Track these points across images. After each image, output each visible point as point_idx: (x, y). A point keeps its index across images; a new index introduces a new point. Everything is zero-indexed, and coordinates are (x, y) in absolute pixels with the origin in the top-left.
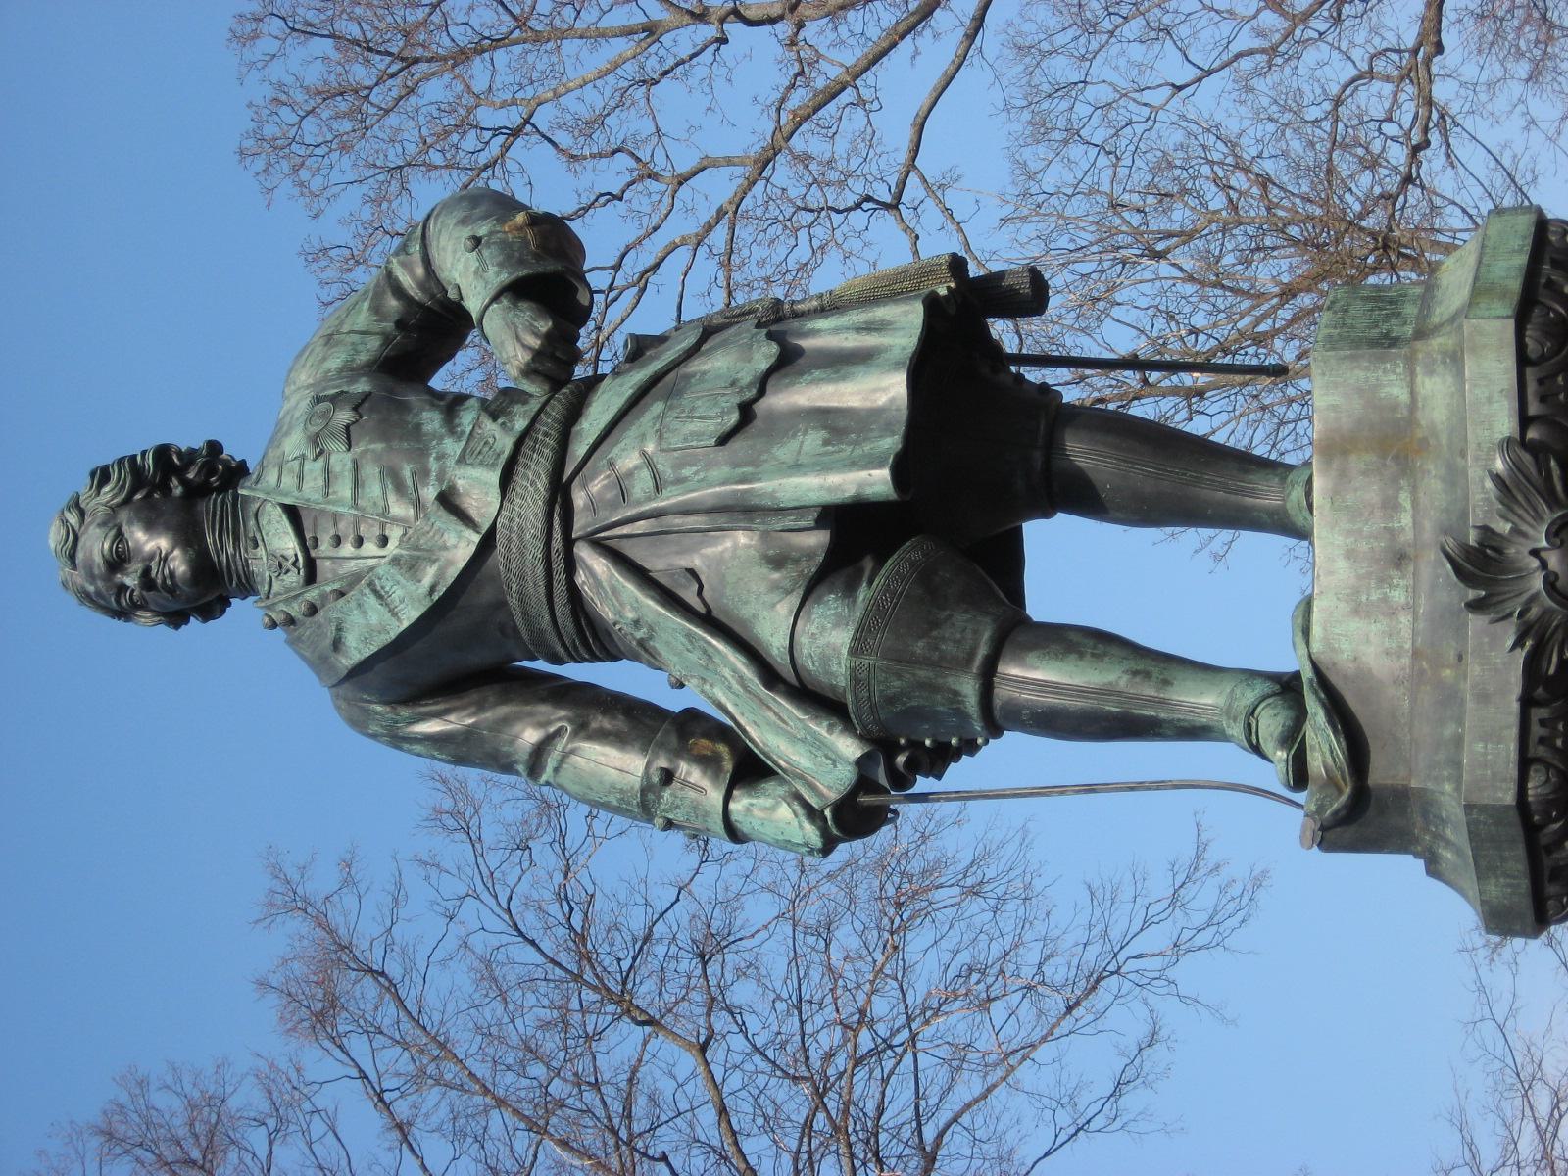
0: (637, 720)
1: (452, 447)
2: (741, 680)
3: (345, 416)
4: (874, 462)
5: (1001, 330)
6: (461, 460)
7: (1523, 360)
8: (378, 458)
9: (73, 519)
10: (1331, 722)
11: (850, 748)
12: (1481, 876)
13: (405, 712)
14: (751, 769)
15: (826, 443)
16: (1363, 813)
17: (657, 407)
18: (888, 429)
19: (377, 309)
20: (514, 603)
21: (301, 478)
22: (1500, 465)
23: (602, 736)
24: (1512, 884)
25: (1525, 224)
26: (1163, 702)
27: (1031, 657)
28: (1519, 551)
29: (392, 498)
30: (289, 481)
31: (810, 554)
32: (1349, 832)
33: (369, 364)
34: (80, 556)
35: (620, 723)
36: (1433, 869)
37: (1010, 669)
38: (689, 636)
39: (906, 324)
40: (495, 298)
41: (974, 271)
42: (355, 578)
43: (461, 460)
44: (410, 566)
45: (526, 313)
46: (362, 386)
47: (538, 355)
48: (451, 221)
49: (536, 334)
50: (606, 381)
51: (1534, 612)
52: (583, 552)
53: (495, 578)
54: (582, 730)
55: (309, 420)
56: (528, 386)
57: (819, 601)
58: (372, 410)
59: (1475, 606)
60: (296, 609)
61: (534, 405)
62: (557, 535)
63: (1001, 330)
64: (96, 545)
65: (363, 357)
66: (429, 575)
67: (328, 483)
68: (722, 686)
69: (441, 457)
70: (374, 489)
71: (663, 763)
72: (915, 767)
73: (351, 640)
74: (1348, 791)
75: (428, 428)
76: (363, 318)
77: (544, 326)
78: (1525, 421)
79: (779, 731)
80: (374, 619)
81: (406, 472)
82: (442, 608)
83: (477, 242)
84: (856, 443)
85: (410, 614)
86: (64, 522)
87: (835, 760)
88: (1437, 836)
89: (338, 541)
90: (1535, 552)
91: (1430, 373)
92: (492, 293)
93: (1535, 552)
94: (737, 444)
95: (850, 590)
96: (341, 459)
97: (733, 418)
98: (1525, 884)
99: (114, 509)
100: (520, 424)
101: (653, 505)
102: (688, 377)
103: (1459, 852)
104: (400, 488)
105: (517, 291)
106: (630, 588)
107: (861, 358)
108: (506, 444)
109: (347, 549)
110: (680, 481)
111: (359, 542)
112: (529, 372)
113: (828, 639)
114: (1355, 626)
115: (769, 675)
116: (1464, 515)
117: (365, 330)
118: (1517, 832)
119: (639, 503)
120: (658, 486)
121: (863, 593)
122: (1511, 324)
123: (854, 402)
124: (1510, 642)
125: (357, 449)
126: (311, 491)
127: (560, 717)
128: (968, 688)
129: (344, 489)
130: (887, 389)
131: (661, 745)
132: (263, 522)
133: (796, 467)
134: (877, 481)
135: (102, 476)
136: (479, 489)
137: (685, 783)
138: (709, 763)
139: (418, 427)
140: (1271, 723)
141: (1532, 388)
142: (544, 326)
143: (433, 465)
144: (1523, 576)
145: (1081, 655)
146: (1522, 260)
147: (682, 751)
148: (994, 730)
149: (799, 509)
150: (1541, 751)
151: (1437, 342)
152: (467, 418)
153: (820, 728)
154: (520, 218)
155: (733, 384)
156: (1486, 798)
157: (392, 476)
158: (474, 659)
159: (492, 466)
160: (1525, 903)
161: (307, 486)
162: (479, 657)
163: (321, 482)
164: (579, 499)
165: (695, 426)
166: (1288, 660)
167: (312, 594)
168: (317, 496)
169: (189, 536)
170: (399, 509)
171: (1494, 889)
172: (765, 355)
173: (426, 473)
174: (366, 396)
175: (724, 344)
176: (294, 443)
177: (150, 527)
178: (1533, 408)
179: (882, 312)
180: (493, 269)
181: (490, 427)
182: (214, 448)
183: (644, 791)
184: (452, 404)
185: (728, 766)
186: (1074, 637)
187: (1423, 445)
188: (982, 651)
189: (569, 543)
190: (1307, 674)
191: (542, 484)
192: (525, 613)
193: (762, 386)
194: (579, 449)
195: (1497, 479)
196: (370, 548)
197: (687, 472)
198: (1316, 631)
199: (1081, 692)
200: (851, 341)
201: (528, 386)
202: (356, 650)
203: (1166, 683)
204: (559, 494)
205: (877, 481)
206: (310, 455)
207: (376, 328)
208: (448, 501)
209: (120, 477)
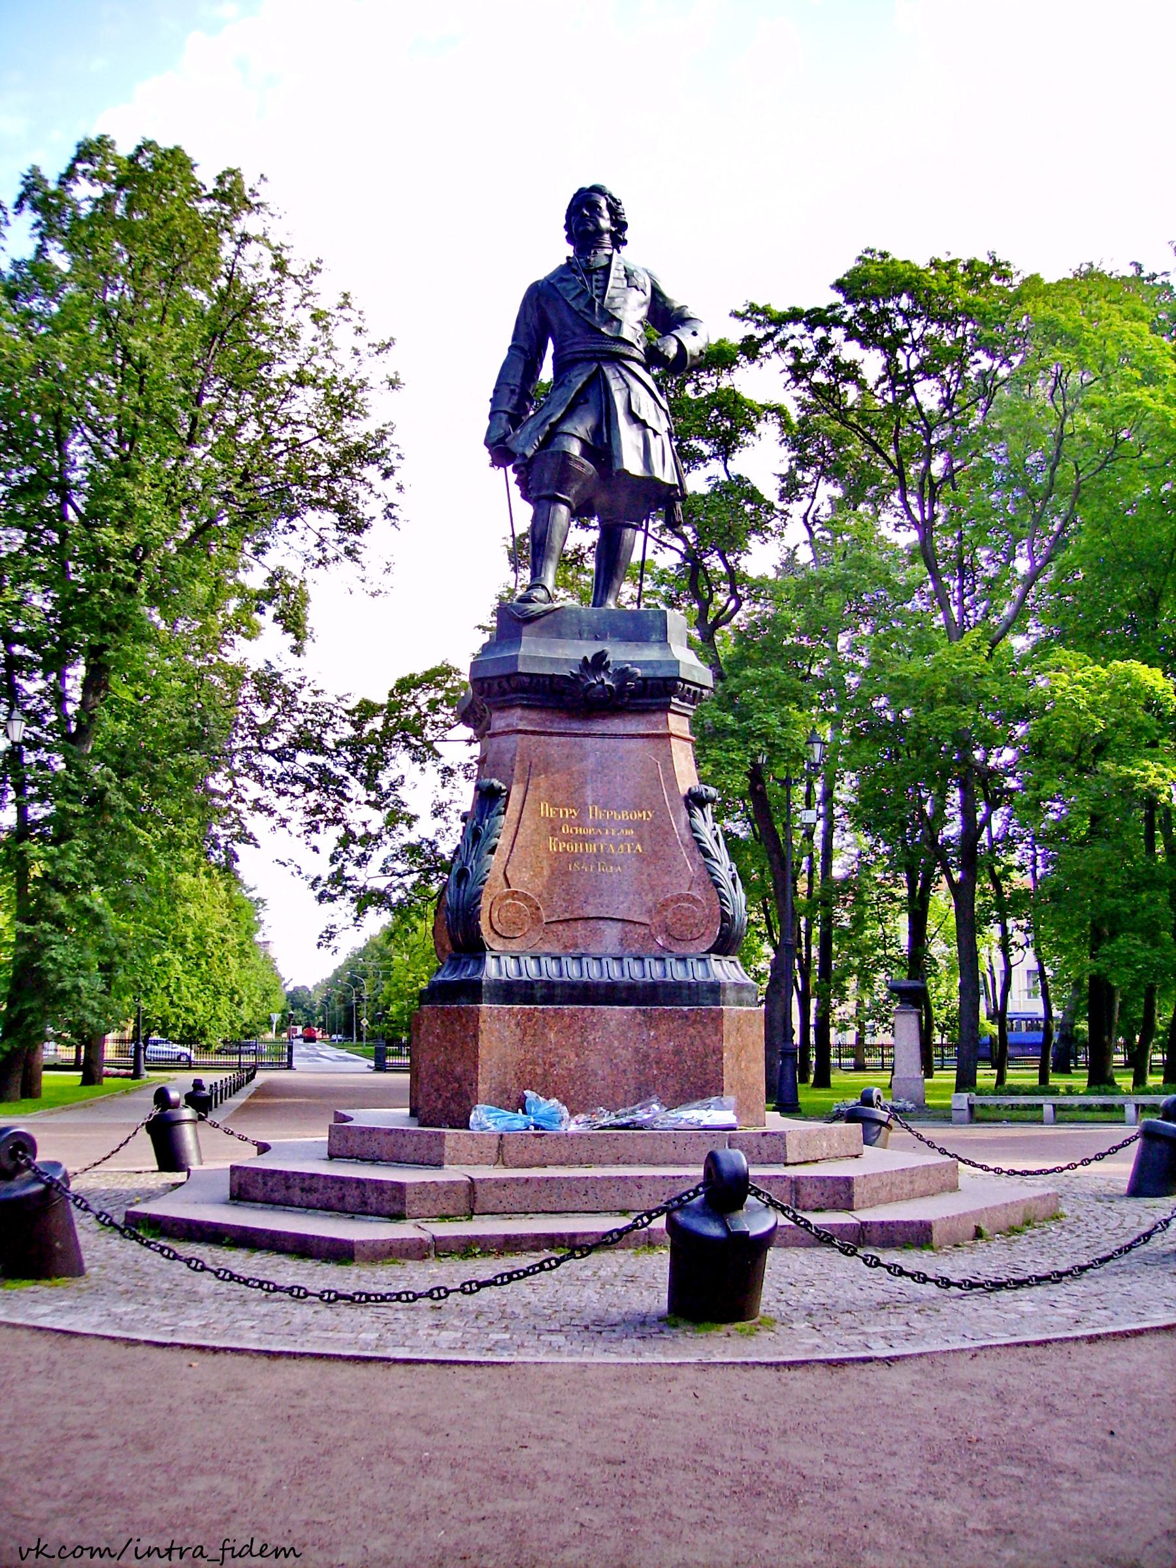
11: (530, 453)
32: (506, 616)
78: (644, 679)
156: (520, 662)
189: (597, 360)
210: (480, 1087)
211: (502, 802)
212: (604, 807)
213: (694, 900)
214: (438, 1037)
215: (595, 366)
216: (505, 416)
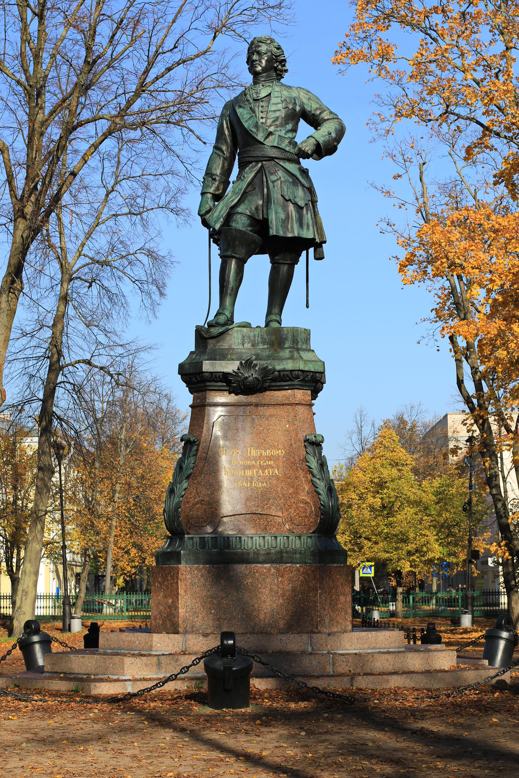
0: (227, 172)
2: (232, 201)
3: (291, 107)
4: (277, 231)
5: (311, 250)
6: (279, 136)
7: (291, 371)
9: (268, 42)
11: (217, 227)
13: (228, 119)
16: (204, 337)
17: (291, 180)
18: (285, 233)
20: (248, 148)
21: (277, 97)
22: (270, 367)
23: (223, 164)
26: (226, 294)
28: (252, 371)
29: (272, 120)
30: (276, 94)
31: (258, 216)
33: (304, 108)
34: (260, 44)
35: (226, 167)
36: (192, 353)
37: (234, 262)
38: (241, 189)
39: (308, 234)
40: (316, 140)
42: (254, 112)
44: (256, 126)
46: (298, 109)
47: (304, 151)
48: (336, 126)
50: (297, 166)
51: (240, 374)
52: (260, 165)
54: (225, 159)
55: (290, 98)
56: (297, 148)
57: (248, 219)
58: (292, 112)
59: (241, 363)
61: (292, 151)
63: (311, 250)
64: (263, 48)
65: (306, 107)
66: (254, 130)
68: (231, 195)
71: (217, 178)
75: (288, 126)
76: (315, 106)
77: (310, 152)
78: (279, 371)
79: (221, 209)
80: (245, 116)
81: (277, 123)
82: (247, 133)
83: (330, 134)
84: (282, 226)
85: (246, 125)
87: (216, 222)
89: (262, 107)
91: (290, 352)
95: (250, 225)
96: (280, 106)
97: (287, 199)
98: (188, 372)
99: (271, 51)
100: (287, 149)
102: (298, 186)
103: (194, 359)
104: (274, 121)
105: (318, 145)
106: (252, 175)
107: (301, 225)
108: (283, 146)
109: (260, 109)
110: (274, 186)
112: (300, 149)
113: (241, 223)
114: (240, 337)
115: (233, 208)
117: (311, 107)
120: (273, 182)
121: (250, 229)
126: (273, 100)
127: (227, 154)
128: (229, 253)
130: (294, 231)
131: (221, 178)
132: (268, 88)
133: (276, 213)
134: (273, 232)
135: (279, 48)
137: (213, 184)
138: (217, 189)
139: (288, 124)
140: (222, 319)
141: (286, 373)
142: (310, 152)
143: (279, 129)
144: (248, 373)
145: (236, 277)
147: (220, 182)
150: (214, 376)
152: (290, 135)
153: (222, 220)
154: (336, 144)
155: (295, 197)
158: (237, 140)
161: (275, 99)
162: (239, 138)
167: (251, 101)
169: (265, 70)
170: (269, 122)
172: (301, 203)
173: (277, 127)
174: (295, 110)
175: (305, 193)
177: (267, 61)
178: (282, 373)
179: (311, 228)
180: (323, 139)
181: (287, 141)
182: (286, 71)
183: (211, 174)
184: (294, 130)
185: (217, 193)
186: (240, 275)
188: (237, 256)
189: (262, 161)
191: (274, 155)
193: (295, 204)
195: (267, 367)
196: (261, 115)
198: (239, 329)
199: (229, 277)
200: (305, 222)
201: (297, 148)
202: (239, 111)
203: (230, 295)
204: (272, 159)
205: (273, 232)
206: (282, 99)
207: (312, 109)
209: (278, 52)
210: (180, 611)
211: (195, 448)
212: (258, 448)
213: (306, 503)
214: (160, 583)
215: (260, 165)
216: (209, 196)
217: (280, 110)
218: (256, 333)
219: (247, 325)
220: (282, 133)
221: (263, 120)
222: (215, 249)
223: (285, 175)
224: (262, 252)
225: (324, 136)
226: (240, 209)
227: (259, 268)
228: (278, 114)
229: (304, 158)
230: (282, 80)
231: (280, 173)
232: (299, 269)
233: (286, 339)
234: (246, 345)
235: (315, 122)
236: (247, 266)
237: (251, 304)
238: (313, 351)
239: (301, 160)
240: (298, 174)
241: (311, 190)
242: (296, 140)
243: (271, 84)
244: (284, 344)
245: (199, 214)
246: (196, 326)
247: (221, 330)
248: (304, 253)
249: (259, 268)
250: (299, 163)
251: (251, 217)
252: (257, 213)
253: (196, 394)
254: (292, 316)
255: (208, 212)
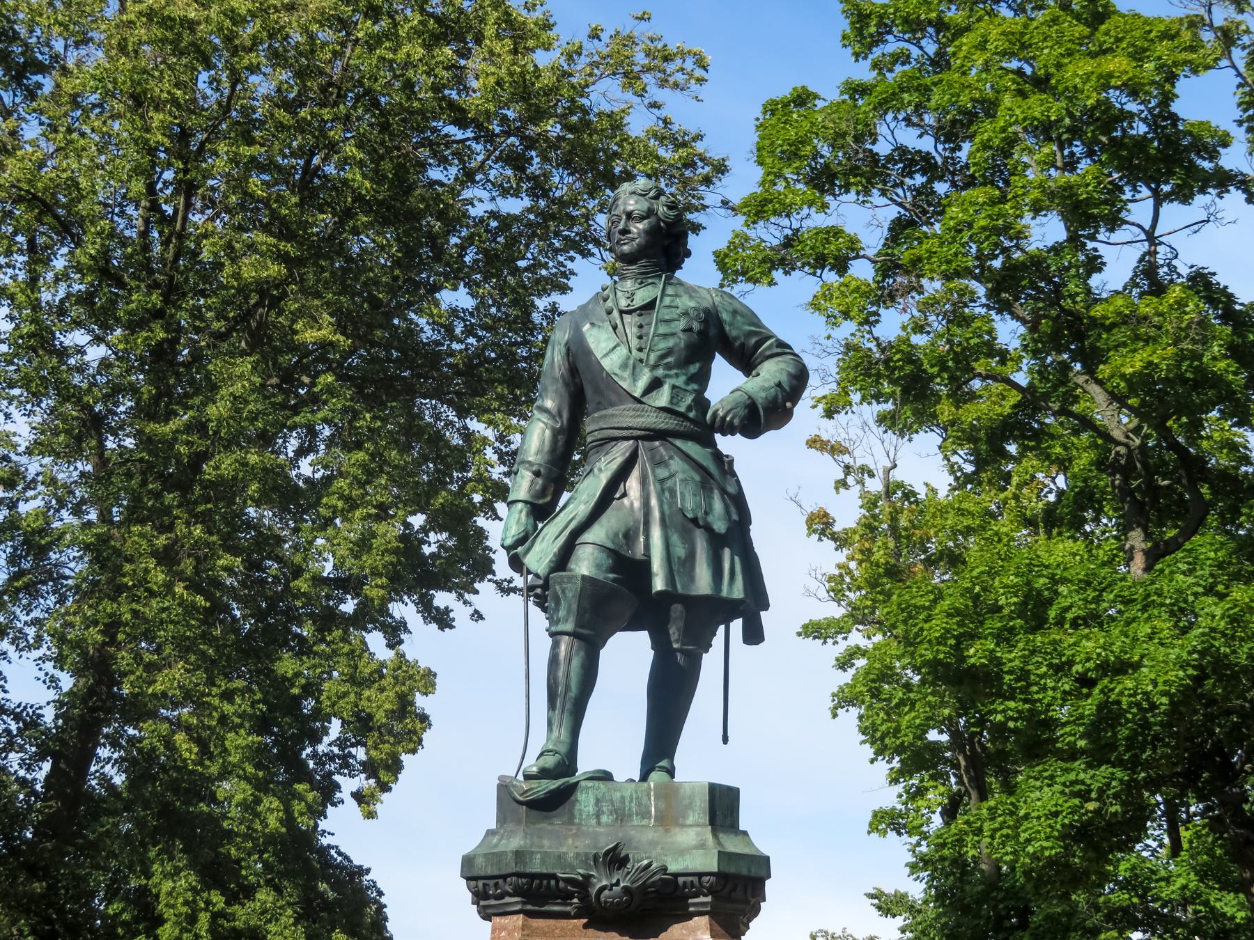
1: (680, 381)
5: (737, 625)
6: (674, 387)
7: (700, 875)
8: (676, 345)
9: (652, 194)
10: (551, 792)
12: (485, 855)
14: (541, 511)
15: (679, 558)
17: (697, 478)
18: (683, 587)
19: (751, 334)
20: (610, 411)
24: (482, 867)
25: (762, 873)
27: (582, 654)
36: (490, 833)
40: (750, 397)
41: (762, 613)
43: (674, 387)
45: (742, 412)
49: (732, 419)
53: (622, 402)
54: (556, 433)
57: (608, 556)
60: (609, 303)
62: (639, 433)
63: (737, 625)
65: (727, 328)
67: (666, 321)
69: (677, 375)
70: (664, 345)
71: (542, 470)
72: (536, 596)
73: (595, 331)
74: (521, 799)
77: (736, 422)
78: (676, 875)
86: (651, 190)
88: (502, 838)
90: (617, 884)
91: (698, 834)
92: (753, 396)
93: (618, 881)
94: (680, 517)
95: (612, 570)
98: (483, 874)
100: (692, 415)
101: (651, 479)
102: (711, 491)
103: (496, 845)
104: (663, 357)
105: (751, 406)
106: (614, 466)
108: (682, 409)
109: (635, 330)
111: (640, 337)
114: (592, 801)
116: (636, 848)
118: (504, 872)
119: (653, 472)
120: (662, 481)
121: (611, 576)
122: (716, 870)
123: (698, 570)
124: (581, 871)
125: (681, 335)
129: (662, 329)
132: (650, 287)
136: (663, 398)
138: (542, 493)
141: (690, 878)
142: (736, 422)
143: (673, 372)
146: (744, 872)
148: (552, 635)
149: (647, 546)
150: (536, 882)
151: (710, 837)
157: (669, 352)
159: (671, 402)
160: (476, 873)
161: (665, 311)
163: (667, 317)
164: (657, 443)
165: (688, 497)
166: (586, 763)
167: (616, 314)
168: (660, 316)
171: (480, 861)
172: (720, 526)
176: (686, 302)
178: (681, 880)
180: (763, 395)
182: (688, 254)
185: (541, 502)
187: (667, 831)
188: (585, 632)
189: (636, 438)
190: (573, 780)
191: (662, 426)
192: (605, 416)
193: (708, 529)
194: (678, 443)
195: (650, 865)
197: (667, 494)
198: (590, 784)
200: (727, 566)
205: (659, 584)
208: (655, 384)
217: (673, 334)
218: (627, 794)
219: (605, 776)
220: (680, 381)
221: (643, 355)
222: (539, 619)
223: (686, 467)
224: (633, 626)
225: (764, 389)
226: (589, 536)
227: (628, 657)
228: (670, 343)
229: (724, 434)
230: (678, 274)
231: (677, 464)
232: (711, 662)
233: (690, 806)
234: (604, 819)
235: (746, 361)
236: (604, 654)
237: (613, 736)
238: (745, 833)
239: (718, 437)
240: (713, 468)
241: (738, 502)
242: (707, 395)
243: (656, 281)
244: (685, 817)
245: (502, 546)
246: (500, 778)
247: (554, 784)
248: (722, 628)
249: (628, 657)
250: (713, 444)
251: (613, 553)
252: (627, 544)
253: (497, 920)
254: (698, 760)
255: (521, 541)
